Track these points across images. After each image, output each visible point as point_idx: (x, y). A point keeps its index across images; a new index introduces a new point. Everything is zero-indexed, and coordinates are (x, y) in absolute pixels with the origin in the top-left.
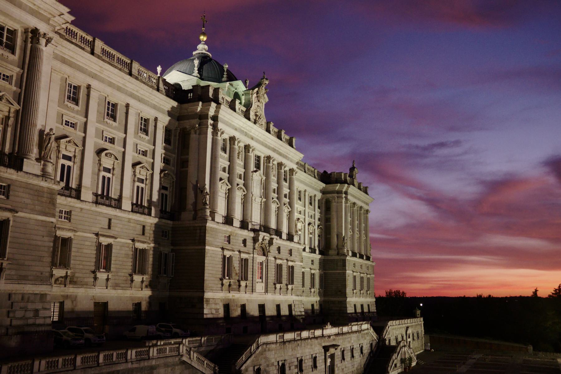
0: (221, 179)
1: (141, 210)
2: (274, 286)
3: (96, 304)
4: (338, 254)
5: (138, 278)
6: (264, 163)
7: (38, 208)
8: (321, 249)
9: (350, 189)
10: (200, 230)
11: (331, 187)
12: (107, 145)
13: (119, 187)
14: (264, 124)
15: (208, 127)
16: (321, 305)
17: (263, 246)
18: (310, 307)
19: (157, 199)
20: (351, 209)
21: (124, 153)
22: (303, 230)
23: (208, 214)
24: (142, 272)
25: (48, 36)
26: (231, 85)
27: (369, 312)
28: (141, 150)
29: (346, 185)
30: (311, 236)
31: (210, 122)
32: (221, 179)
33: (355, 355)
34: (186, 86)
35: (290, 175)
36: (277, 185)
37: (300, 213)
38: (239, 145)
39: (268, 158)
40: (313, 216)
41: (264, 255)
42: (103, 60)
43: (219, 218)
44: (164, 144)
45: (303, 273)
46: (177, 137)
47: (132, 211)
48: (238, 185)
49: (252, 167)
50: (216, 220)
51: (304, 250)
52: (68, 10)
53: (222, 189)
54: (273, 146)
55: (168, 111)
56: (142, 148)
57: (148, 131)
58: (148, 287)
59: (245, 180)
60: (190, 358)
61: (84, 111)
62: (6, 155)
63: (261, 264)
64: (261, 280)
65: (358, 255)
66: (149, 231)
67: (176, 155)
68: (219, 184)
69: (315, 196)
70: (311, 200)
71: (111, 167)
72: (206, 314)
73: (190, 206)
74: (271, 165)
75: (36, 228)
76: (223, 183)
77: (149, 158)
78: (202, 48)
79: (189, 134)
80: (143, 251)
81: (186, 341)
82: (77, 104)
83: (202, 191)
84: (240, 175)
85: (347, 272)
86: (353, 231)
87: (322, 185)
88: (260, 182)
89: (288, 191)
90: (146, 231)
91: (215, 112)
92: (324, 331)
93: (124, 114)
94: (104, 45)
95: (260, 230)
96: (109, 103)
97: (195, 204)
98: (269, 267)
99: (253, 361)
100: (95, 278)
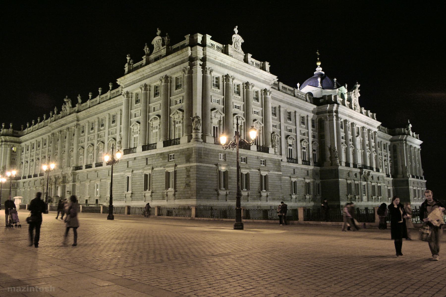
0: (342, 143)
4: (403, 177)
5: (308, 197)
9: (408, 138)
11: (396, 137)
12: (289, 133)
21: (296, 136)
23: (338, 162)
24: (310, 194)
25: (270, 91)
29: (405, 136)
30: (386, 167)
31: (334, 114)
32: (342, 143)
36: (368, 142)
39: (363, 128)
41: (365, 181)
42: (283, 92)
43: (343, 164)
49: (356, 135)
50: (342, 165)
53: (343, 148)
55: (312, 111)
56: (303, 132)
63: (364, 186)
64: (365, 195)
65: (415, 177)
69: (387, 143)
73: (328, 159)
74: (365, 131)
75: (276, 177)
78: (319, 70)
80: (309, 184)
82: (276, 116)
83: (334, 151)
84: (350, 139)
85: (410, 187)
86: (411, 162)
89: (374, 144)
90: (309, 173)
97: (331, 158)
100: (292, 198)
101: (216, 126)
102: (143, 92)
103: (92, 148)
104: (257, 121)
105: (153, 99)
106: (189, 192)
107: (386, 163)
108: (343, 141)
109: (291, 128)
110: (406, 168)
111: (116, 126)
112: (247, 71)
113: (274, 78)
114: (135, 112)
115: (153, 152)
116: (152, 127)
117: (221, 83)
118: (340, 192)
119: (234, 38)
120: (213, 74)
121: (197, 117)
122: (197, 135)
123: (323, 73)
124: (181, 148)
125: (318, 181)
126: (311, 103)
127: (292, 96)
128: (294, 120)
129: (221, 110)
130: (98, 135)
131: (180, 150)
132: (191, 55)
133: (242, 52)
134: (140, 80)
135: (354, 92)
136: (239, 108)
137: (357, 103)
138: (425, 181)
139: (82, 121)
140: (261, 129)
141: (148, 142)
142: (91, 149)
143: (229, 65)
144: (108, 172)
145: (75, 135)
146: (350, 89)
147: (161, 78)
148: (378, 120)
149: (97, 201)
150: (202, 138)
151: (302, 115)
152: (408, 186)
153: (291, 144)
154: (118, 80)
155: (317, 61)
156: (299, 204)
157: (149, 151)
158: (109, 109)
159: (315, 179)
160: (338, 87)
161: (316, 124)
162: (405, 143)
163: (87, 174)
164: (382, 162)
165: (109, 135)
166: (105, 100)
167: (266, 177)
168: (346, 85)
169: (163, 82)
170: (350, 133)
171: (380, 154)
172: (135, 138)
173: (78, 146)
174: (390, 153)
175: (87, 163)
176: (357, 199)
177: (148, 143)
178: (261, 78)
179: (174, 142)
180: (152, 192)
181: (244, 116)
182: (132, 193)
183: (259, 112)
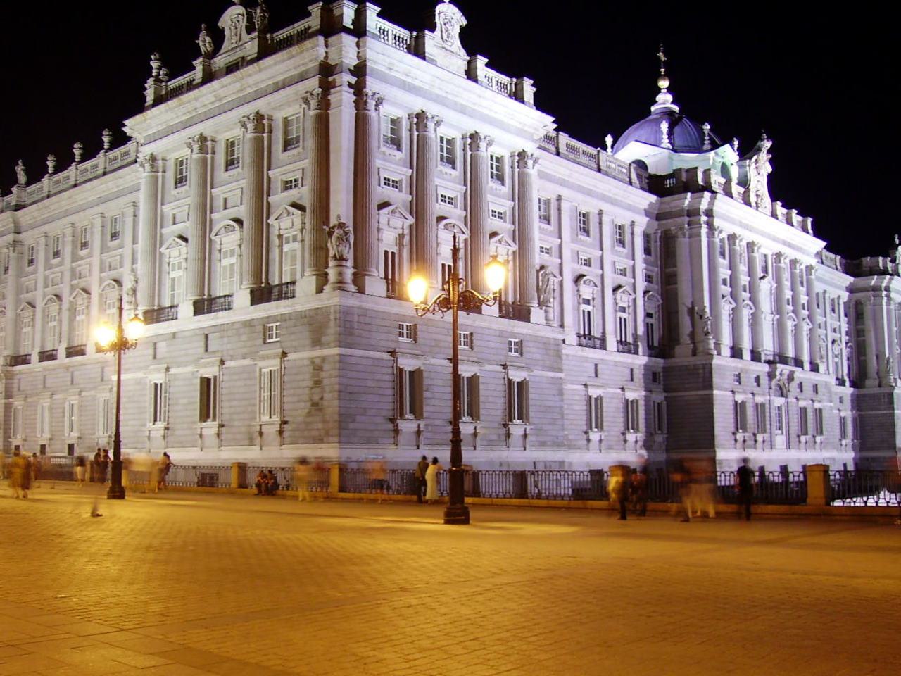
0: (723, 297)
2: (797, 439)
4: (880, 386)
5: (631, 437)
6: (772, 266)
7: (548, 363)
9: (893, 282)
10: (704, 368)
11: (862, 282)
12: (584, 270)
13: (601, 322)
15: (701, 227)
16: (856, 465)
17: (781, 383)
20: (895, 313)
21: (602, 276)
23: (712, 346)
24: (636, 430)
26: (717, 154)
29: (888, 277)
30: (836, 360)
31: (704, 218)
32: (723, 297)
35: (807, 275)
36: (791, 293)
39: (778, 256)
40: (837, 330)
41: (782, 395)
42: (569, 160)
43: (726, 351)
44: (644, 256)
46: (658, 243)
47: (618, 351)
52: (553, 119)
53: (726, 308)
55: (645, 210)
56: (620, 267)
57: (624, 241)
61: (557, 231)
62: (510, 305)
63: (779, 408)
64: (780, 432)
66: (639, 374)
67: (659, 268)
69: (839, 297)
70: (833, 305)
71: (590, 298)
73: (685, 339)
74: (782, 265)
78: (665, 100)
83: (701, 317)
88: (769, 292)
89: (807, 298)
90: (635, 376)
91: (709, 205)
93: (598, 224)
94: (570, 139)
97: (692, 335)
98: (790, 412)
100: (588, 440)
101: (390, 251)
102: (195, 156)
103: (58, 307)
104: (499, 237)
105: (221, 174)
106: (320, 426)
107: (836, 348)
108: (726, 290)
109: (589, 256)
110: (888, 362)
111: (121, 247)
112: (474, 104)
113: (546, 122)
114: (174, 212)
115: (221, 318)
116: (220, 251)
117: (405, 134)
119: (439, 14)
120: (384, 109)
121: (341, 226)
122: (340, 274)
123: (676, 108)
124: (299, 308)
125: (659, 397)
126: (642, 188)
129: (403, 206)
130: (73, 270)
131: (297, 312)
132: (326, 57)
133: (463, 52)
134: (187, 125)
135: (756, 162)
136: (451, 201)
139: (29, 233)
140: (511, 258)
141: (209, 290)
142: (54, 308)
143: (426, 87)
144: (100, 370)
145: (10, 271)
146: (746, 152)
147: (245, 119)
148: (817, 234)
149: (71, 447)
150: (355, 282)
151: (619, 222)
152: (893, 409)
153: (589, 297)
154: (126, 122)
155: (658, 76)
157: (213, 314)
158: (102, 201)
159: (650, 391)
160: (715, 146)
162: (886, 296)
163: (45, 377)
164: (827, 346)
165: (102, 271)
166: (90, 177)
167: (521, 385)
168: (736, 143)
169: (249, 132)
170: (743, 268)
171: (822, 325)
172: (173, 279)
173: (18, 302)
175: (42, 346)
176: (759, 444)
177: (209, 295)
178: (511, 122)
179: (281, 292)
180: (222, 426)
181: (466, 225)
182: (167, 429)
183: (505, 212)
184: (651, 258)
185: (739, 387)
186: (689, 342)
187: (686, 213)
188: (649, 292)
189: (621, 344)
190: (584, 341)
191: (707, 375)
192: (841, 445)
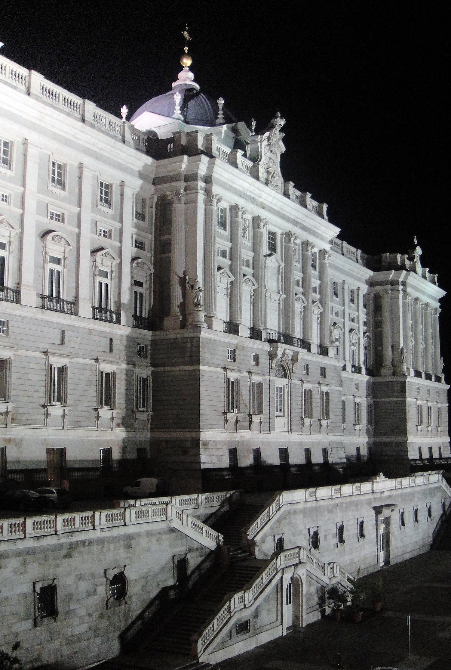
0: (219, 268)
1: (105, 316)
3: (50, 451)
4: (394, 374)
5: (105, 413)
6: (282, 243)
8: (368, 367)
9: (409, 277)
10: (192, 342)
11: (381, 276)
12: (54, 225)
13: (73, 285)
14: (280, 185)
15: (198, 192)
16: (370, 449)
18: (355, 453)
19: (128, 301)
21: (79, 235)
22: (341, 341)
27: (441, 458)
28: (103, 229)
29: (404, 272)
30: (353, 348)
31: (201, 184)
33: (419, 518)
34: (163, 134)
35: (320, 259)
36: (301, 275)
37: (337, 314)
38: (245, 216)
39: (288, 235)
40: (356, 319)
41: (285, 376)
43: (219, 325)
45: (344, 403)
46: (154, 209)
47: (94, 318)
48: (244, 275)
49: (265, 249)
51: (344, 368)
54: (293, 218)
58: (121, 425)
59: (233, 258)
60: (183, 524)
64: (281, 414)
65: (423, 375)
66: (120, 347)
68: (218, 275)
69: (358, 289)
70: (352, 296)
72: (204, 463)
73: (176, 310)
74: (292, 245)
76: (223, 273)
77: (115, 240)
79: (171, 203)
81: (176, 500)
83: (192, 287)
84: (248, 262)
85: (408, 399)
86: (416, 340)
87: (368, 273)
88: (276, 271)
89: (319, 282)
90: (114, 347)
92: (375, 485)
95: (279, 341)
96: (54, 164)
97: (183, 306)
98: (293, 394)
99: (272, 528)
100: (47, 415)
109: (63, 211)
110: (402, 352)
118: (202, 403)
123: (197, 87)
126: (138, 149)
127: (76, 118)
128: (77, 190)
137: (277, 168)
138: (448, 387)
148: (333, 219)
152: (405, 396)
155: (182, 54)
156: (72, 433)
159: (134, 365)
161: (151, 213)
168: (254, 124)
170: (246, 242)
174: (367, 314)
184: (146, 224)
185: (234, 364)
186: (179, 314)
187: (182, 178)
188: (139, 258)
189: (100, 311)
190: (48, 304)
191: (195, 349)
192: (355, 430)
